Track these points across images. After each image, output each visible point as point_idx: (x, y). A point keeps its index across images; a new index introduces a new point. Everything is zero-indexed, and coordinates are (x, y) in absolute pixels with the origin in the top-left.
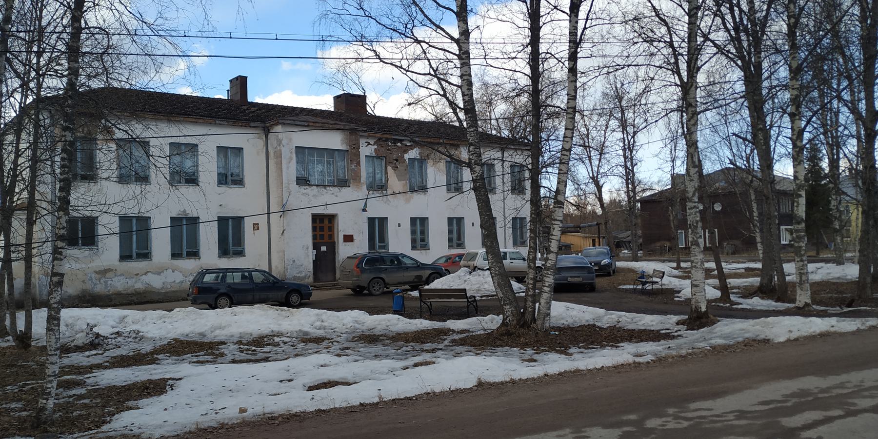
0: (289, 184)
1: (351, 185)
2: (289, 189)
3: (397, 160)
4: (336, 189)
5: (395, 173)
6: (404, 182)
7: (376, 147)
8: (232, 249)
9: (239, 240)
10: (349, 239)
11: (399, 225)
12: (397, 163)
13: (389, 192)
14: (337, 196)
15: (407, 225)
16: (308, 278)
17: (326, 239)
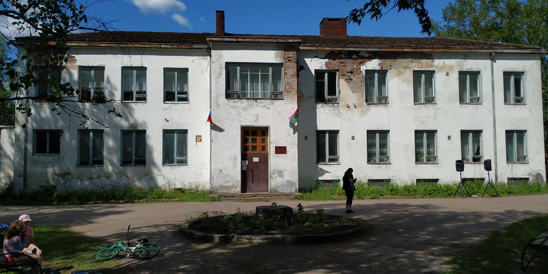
0: (218, 98)
1: (285, 97)
2: (217, 102)
3: (352, 73)
4: (268, 101)
5: (349, 85)
6: (360, 94)
7: (327, 60)
8: (176, 158)
9: (183, 151)
10: (281, 150)
11: (353, 138)
12: (352, 75)
13: (342, 104)
14: (268, 108)
16: (235, 188)
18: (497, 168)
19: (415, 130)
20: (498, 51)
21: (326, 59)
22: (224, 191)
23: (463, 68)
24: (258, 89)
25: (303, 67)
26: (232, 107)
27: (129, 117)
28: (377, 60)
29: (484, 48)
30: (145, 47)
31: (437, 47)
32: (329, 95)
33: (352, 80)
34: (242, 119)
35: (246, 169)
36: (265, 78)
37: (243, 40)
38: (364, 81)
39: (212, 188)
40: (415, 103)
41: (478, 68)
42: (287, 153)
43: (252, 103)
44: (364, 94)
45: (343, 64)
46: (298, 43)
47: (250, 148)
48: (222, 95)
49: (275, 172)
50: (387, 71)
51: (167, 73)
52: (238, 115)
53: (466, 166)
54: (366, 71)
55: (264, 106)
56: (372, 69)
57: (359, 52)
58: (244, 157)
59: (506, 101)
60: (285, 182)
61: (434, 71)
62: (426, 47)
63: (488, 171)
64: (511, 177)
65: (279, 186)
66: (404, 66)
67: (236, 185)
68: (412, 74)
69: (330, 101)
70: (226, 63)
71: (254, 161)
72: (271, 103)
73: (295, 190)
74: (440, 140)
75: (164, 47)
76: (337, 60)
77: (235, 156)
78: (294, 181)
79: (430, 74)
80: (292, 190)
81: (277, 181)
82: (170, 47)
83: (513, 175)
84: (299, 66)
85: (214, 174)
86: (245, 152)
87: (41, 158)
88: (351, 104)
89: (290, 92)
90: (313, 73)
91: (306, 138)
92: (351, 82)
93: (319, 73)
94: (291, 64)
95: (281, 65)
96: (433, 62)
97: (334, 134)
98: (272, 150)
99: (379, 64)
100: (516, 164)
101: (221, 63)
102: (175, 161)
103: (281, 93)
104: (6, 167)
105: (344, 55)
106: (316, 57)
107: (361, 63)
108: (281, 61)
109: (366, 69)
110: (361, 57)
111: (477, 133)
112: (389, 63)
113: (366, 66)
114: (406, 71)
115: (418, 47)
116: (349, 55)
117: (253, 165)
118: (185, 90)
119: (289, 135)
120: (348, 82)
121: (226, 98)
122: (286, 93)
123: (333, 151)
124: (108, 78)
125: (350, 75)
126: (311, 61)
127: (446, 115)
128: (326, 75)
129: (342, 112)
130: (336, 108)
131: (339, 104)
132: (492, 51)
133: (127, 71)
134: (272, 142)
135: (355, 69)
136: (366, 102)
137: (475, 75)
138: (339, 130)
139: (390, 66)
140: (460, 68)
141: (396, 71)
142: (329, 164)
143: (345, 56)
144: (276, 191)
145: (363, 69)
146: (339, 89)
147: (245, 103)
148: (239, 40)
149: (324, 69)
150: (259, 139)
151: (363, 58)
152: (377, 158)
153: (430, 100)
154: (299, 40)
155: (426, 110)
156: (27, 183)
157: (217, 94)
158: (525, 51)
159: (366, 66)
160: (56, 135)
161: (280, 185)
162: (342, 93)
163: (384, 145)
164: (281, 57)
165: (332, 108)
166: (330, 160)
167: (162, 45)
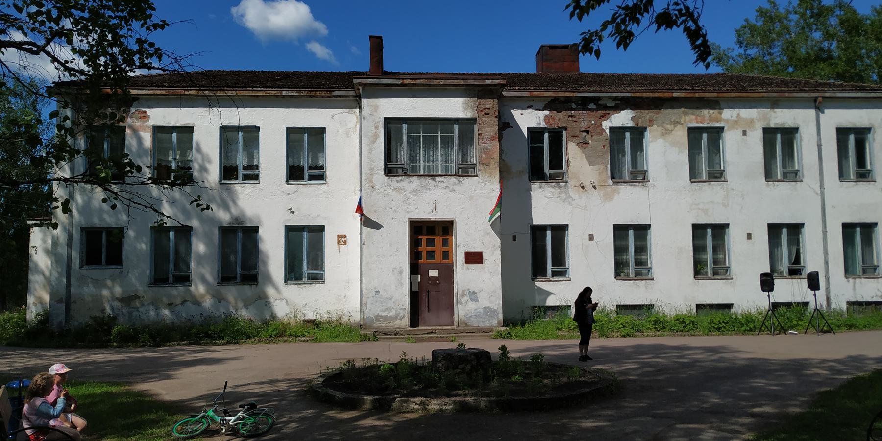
0: (372, 175)
1: (479, 173)
2: (371, 181)
3: (588, 132)
4: (453, 179)
5: (583, 152)
6: (602, 167)
7: (547, 112)
8: (306, 271)
9: (317, 260)
10: (474, 258)
11: (591, 237)
13: (572, 182)
14: (453, 191)
15: (608, 238)
16: (401, 319)
17: (438, 257)
18: (829, 286)
19: (693, 225)
20: (827, 94)
21: (545, 111)
22: (383, 325)
23: (771, 123)
24: (437, 160)
25: (509, 123)
26: (395, 189)
27: (231, 204)
28: (629, 111)
29: (805, 90)
30: (257, 96)
31: (727, 90)
32: (551, 168)
33: (588, 143)
34: (412, 208)
35: (417, 289)
36: (447, 142)
37: (412, 83)
38: (608, 145)
39: (363, 319)
40: (693, 180)
41: (795, 123)
42: (483, 262)
43: (427, 182)
44: (609, 166)
45: (574, 119)
46: (500, 86)
47: (424, 254)
48: (378, 170)
49: (465, 293)
50: (645, 129)
51: (292, 136)
52: (404, 202)
53: (778, 283)
54: (611, 128)
55: (447, 187)
56: (621, 126)
57: (599, 98)
58: (414, 269)
59: (842, 176)
60: (481, 310)
61: (722, 129)
62: (708, 90)
63: (813, 291)
64: (853, 300)
65: (471, 316)
66: (672, 120)
67: (401, 314)
68: (686, 133)
69: (553, 178)
70: (385, 119)
71: (430, 276)
72: (457, 182)
73: (497, 322)
74: (735, 240)
75: (287, 94)
76: (564, 112)
77: (401, 267)
78: (496, 309)
79: (716, 134)
80: (492, 323)
81: (469, 309)
82: (296, 94)
83: (856, 298)
84: (502, 123)
85: (366, 297)
86: (415, 262)
87: (93, 272)
88: (587, 183)
89: (488, 164)
90: (526, 134)
91: (514, 238)
92: (587, 146)
93: (535, 134)
94: (489, 119)
95: (472, 121)
96: (721, 113)
97: (560, 231)
98: (459, 258)
99: (632, 119)
100: (861, 278)
101: (377, 120)
102: (305, 276)
103: (474, 166)
104: (37, 286)
105: (575, 104)
106: (530, 107)
107: (603, 117)
108: (473, 115)
109: (611, 126)
110: (602, 107)
111: (795, 229)
112: (648, 116)
113: (611, 121)
114: (676, 128)
115: (695, 89)
116: (583, 104)
117: (429, 283)
118: (321, 162)
119: (488, 234)
120: (582, 147)
121: (385, 174)
122: (481, 165)
123: (559, 258)
124: (198, 144)
125: (585, 136)
126: (522, 114)
127: (743, 199)
128: (546, 135)
129: (573, 197)
130: (563, 190)
131: (567, 182)
132: (817, 96)
133: (227, 132)
134: (460, 245)
135: (593, 126)
136: (611, 180)
137: (789, 134)
138: (568, 225)
139: (650, 121)
140: (766, 123)
141: (660, 129)
142: (553, 279)
143: (577, 106)
144: (466, 325)
145: (606, 127)
146: (567, 159)
147: (415, 182)
148: (405, 83)
149: (542, 126)
150: (438, 240)
151: (606, 108)
152: (631, 269)
153: (717, 175)
154: (502, 80)
155: (711, 192)
156: (72, 312)
157: (372, 169)
158: (872, 93)
159: (611, 121)
160: (116, 236)
161: (473, 314)
162: (572, 164)
163: (641, 249)
164: (472, 108)
165: (557, 189)
166: (554, 274)
167: (284, 92)
